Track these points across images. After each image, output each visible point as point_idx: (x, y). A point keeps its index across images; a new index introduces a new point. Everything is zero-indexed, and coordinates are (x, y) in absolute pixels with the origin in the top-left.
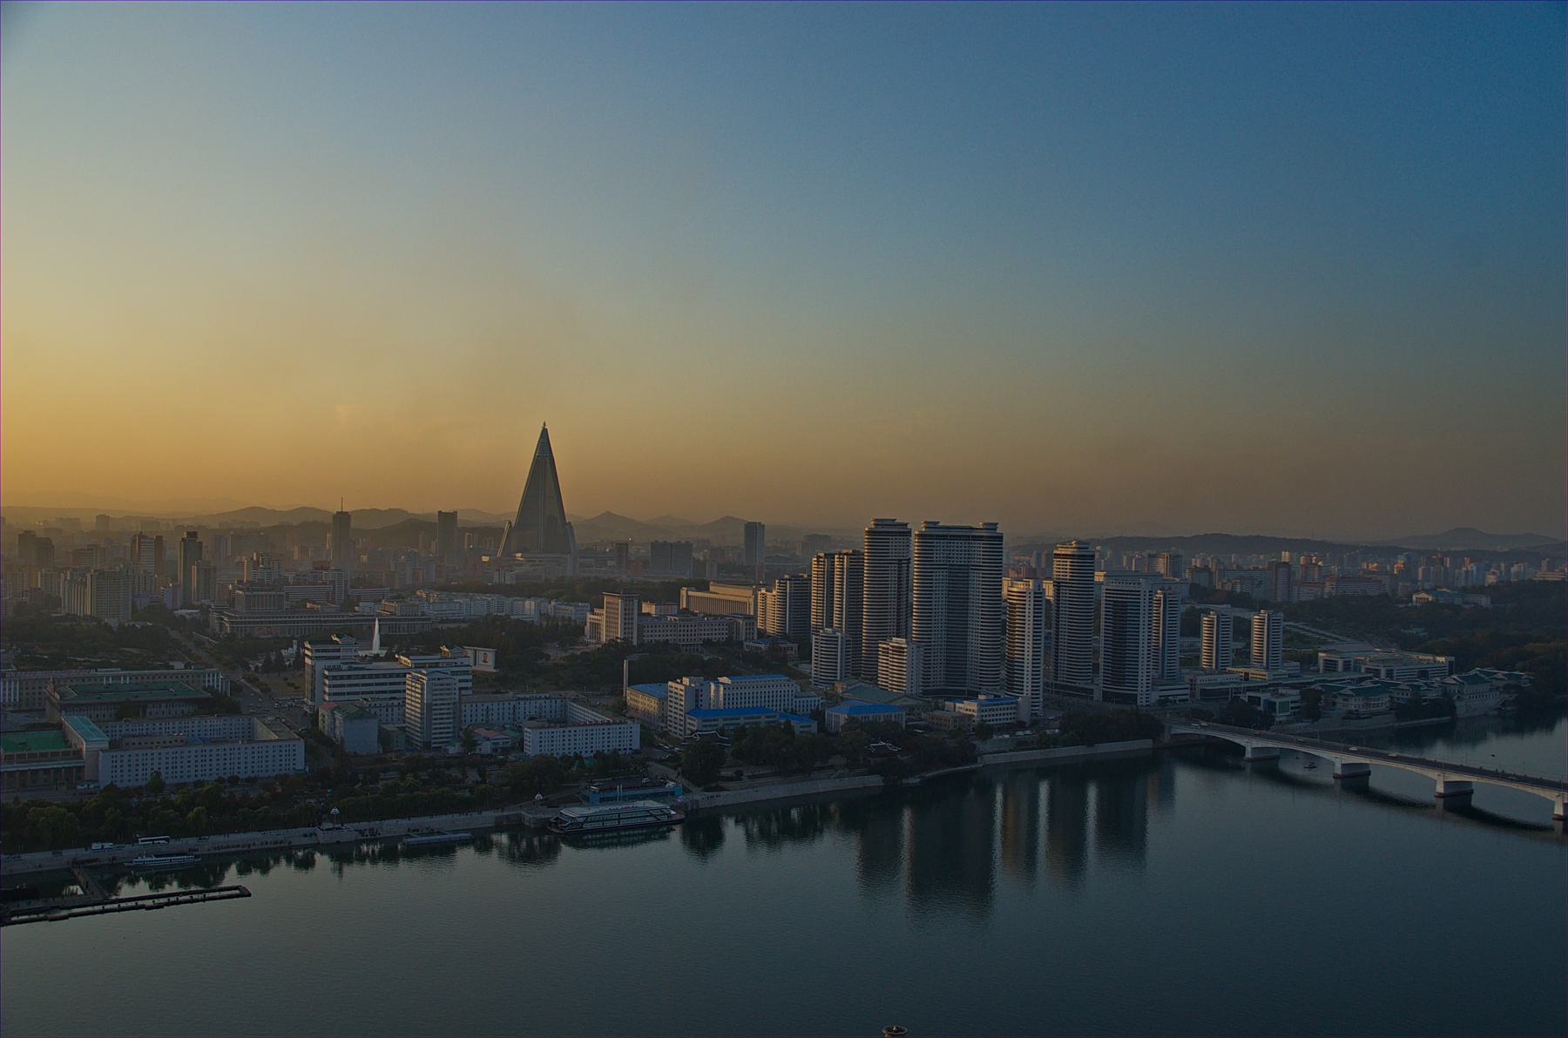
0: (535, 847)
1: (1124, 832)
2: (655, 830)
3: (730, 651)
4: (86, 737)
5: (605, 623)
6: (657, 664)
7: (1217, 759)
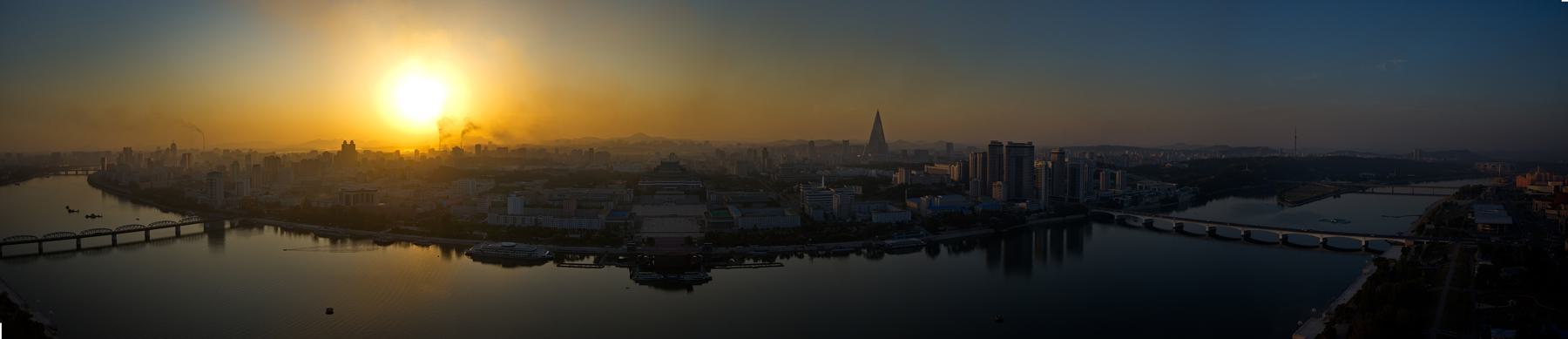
0: (876, 253)
1: (1076, 245)
2: (917, 248)
3: (942, 186)
4: (735, 213)
5: (899, 177)
6: (917, 191)
7: (1106, 220)
